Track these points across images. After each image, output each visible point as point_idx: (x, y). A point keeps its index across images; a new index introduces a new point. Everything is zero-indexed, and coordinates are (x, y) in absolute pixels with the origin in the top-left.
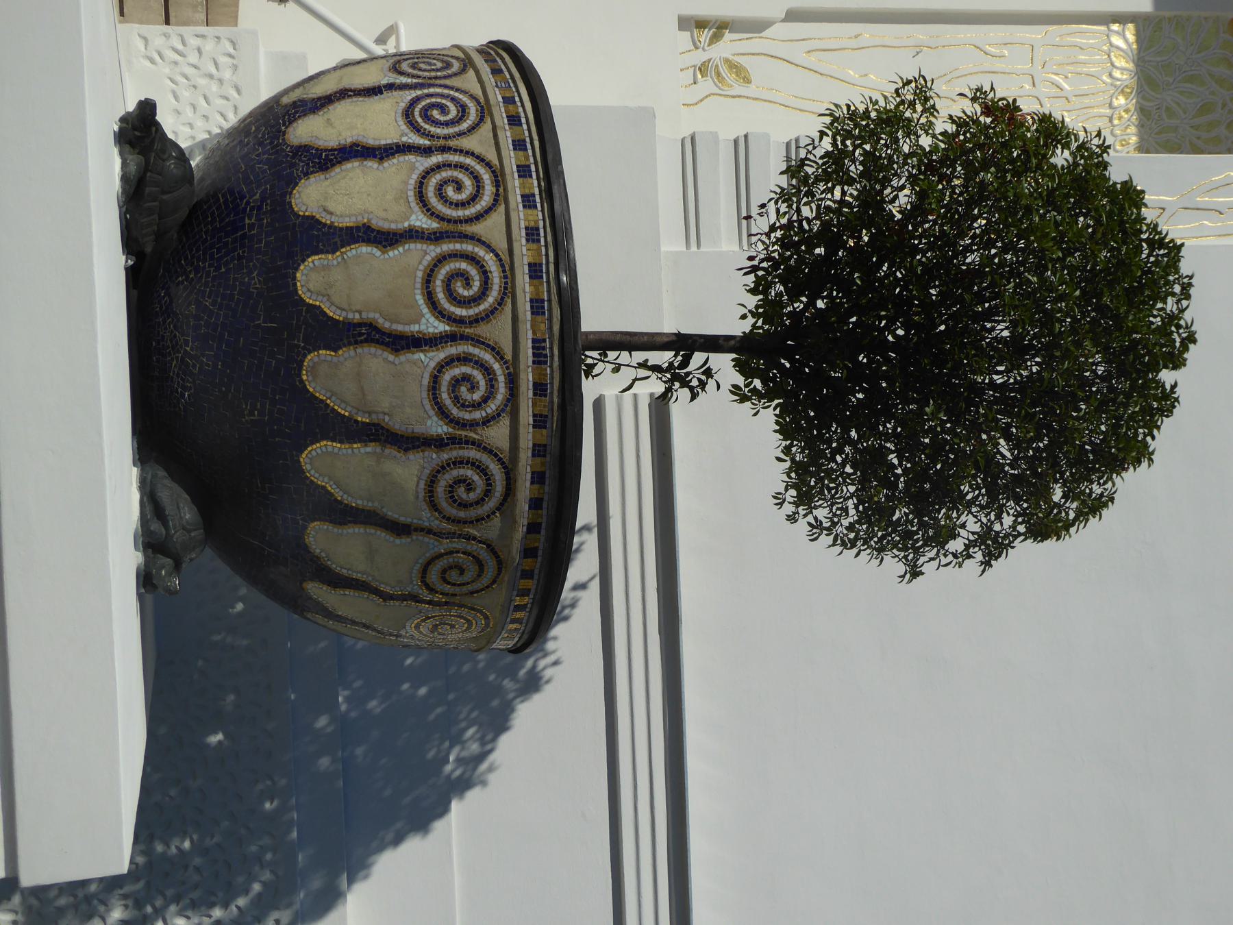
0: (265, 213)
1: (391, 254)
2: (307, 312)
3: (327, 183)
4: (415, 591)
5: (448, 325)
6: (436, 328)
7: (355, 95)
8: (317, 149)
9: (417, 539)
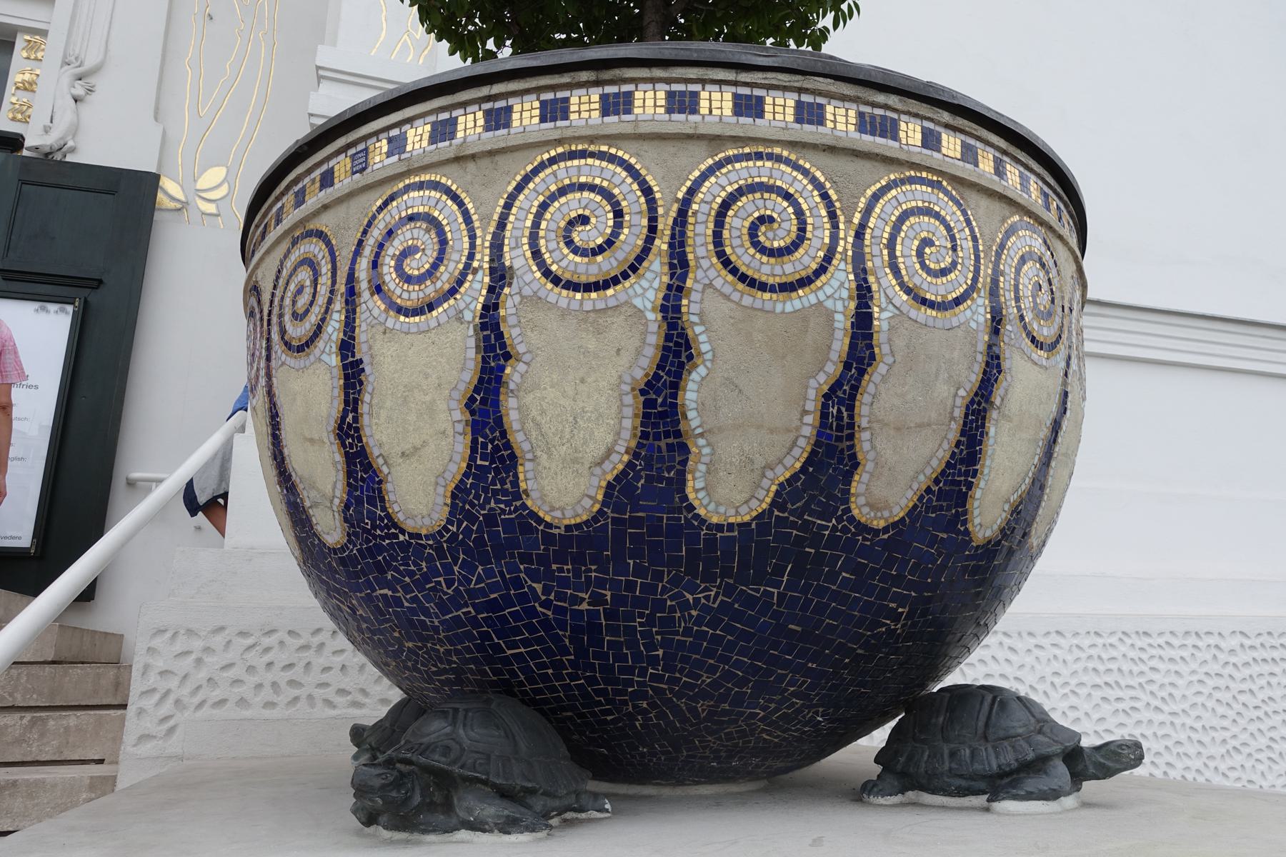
0: (577, 574)
1: (705, 348)
2: (783, 510)
3: (544, 458)
7: (355, 410)
8: (466, 475)
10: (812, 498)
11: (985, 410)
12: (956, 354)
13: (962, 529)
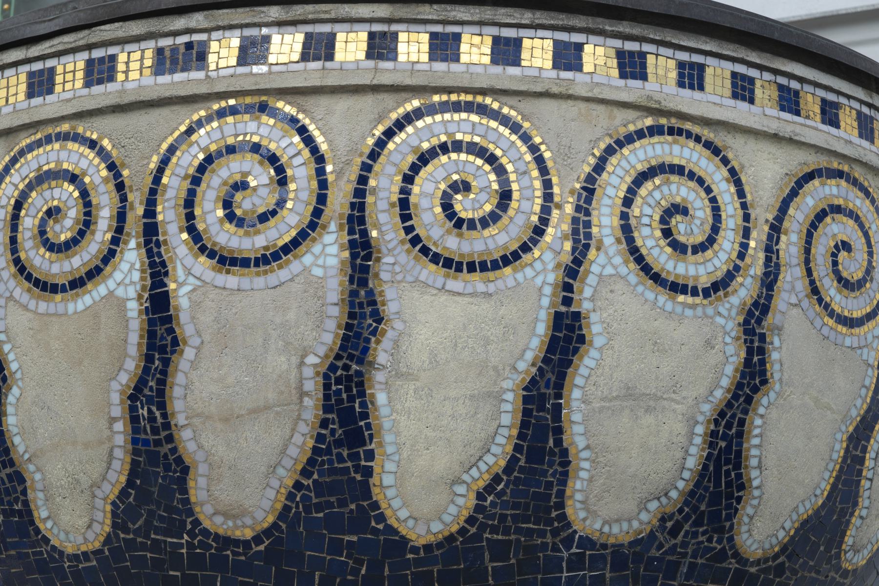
1: (14, 366)
2: (126, 531)
4: (734, 312)
5: (126, 243)
6: (132, 265)
9: (592, 299)
10: (151, 513)
11: (359, 374)
12: (291, 316)
13: (381, 527)
